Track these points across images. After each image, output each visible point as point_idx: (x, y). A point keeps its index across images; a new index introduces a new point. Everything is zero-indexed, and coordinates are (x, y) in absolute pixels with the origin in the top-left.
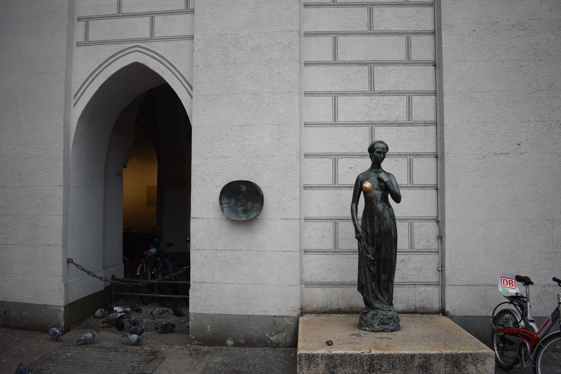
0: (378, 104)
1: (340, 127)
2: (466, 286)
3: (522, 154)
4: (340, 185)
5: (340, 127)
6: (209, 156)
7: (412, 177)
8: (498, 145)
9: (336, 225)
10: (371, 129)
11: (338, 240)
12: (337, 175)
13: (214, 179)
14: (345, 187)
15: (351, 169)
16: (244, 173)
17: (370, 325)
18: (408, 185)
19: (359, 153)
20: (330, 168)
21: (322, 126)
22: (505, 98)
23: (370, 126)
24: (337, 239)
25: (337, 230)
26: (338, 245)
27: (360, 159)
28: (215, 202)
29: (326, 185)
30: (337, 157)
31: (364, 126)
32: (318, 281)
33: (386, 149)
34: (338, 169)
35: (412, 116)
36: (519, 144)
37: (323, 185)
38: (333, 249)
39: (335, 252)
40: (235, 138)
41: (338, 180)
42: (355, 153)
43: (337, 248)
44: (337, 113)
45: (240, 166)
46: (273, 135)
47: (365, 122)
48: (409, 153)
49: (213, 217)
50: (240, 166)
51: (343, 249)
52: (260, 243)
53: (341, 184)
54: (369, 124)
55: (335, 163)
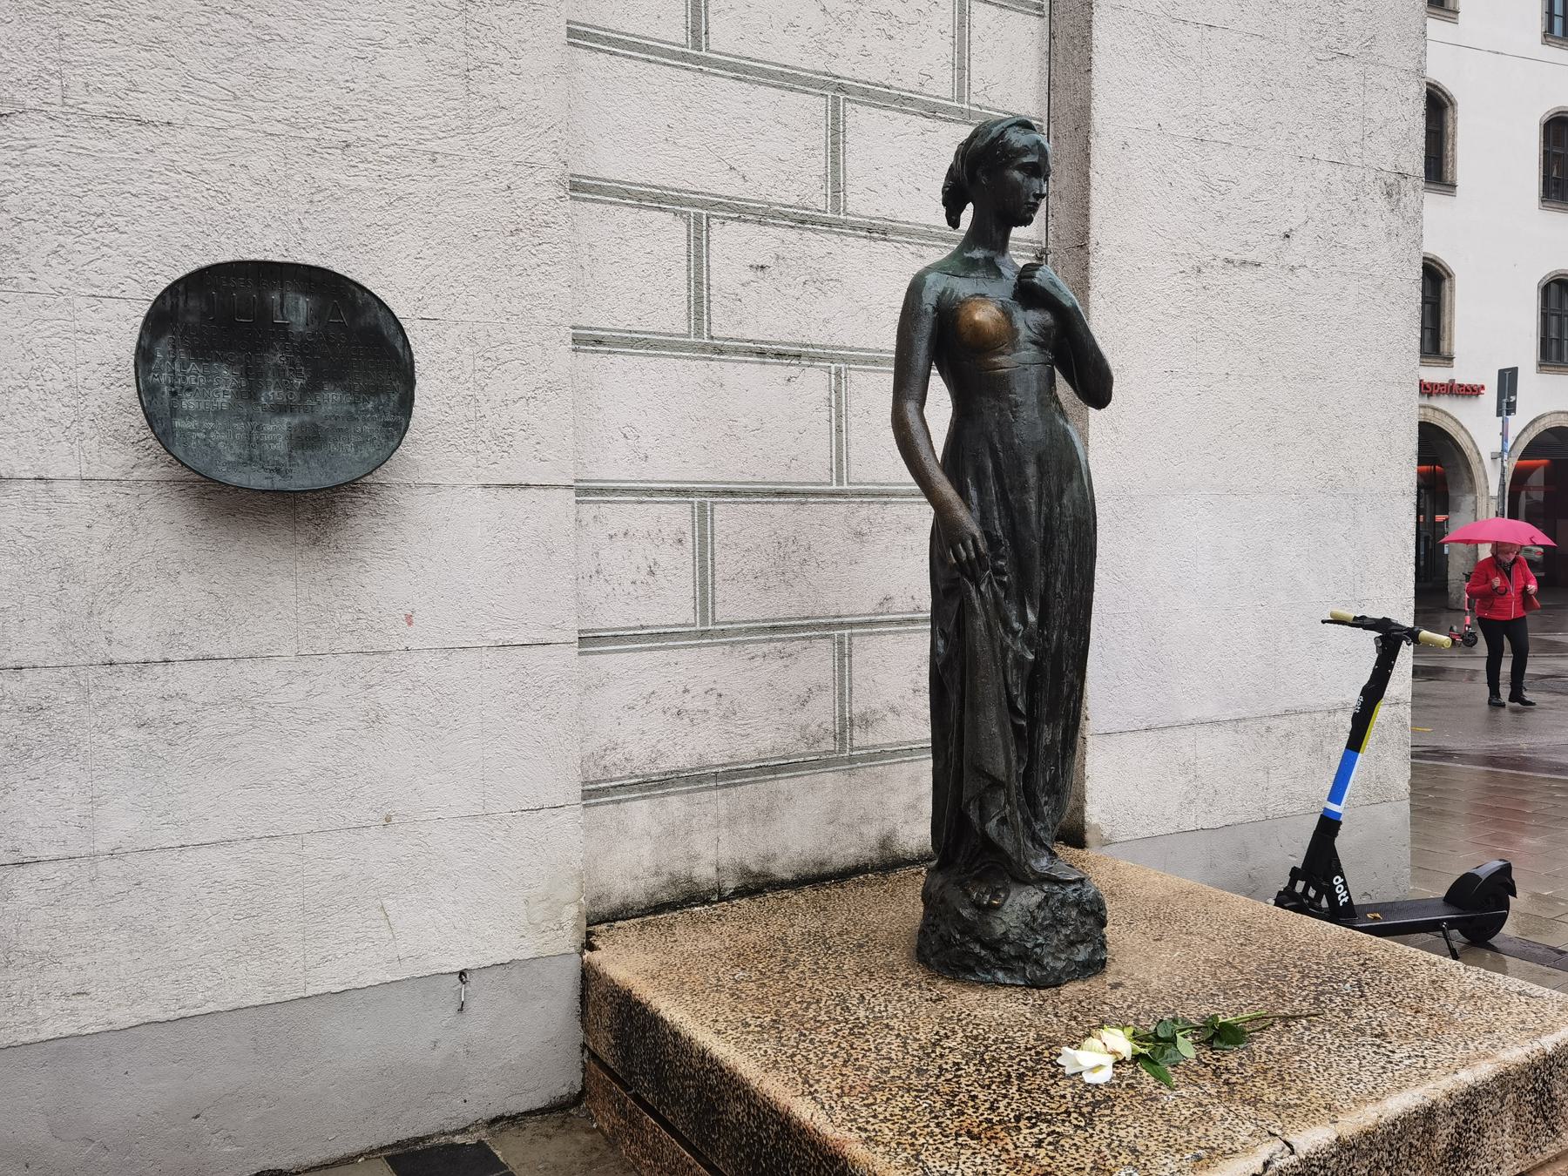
0: (858, 6)
1: (716, 75)
2: (1143, 733)
3: (1292, 269)
5: (716, 75)
6: (31, 103)
8: (1236, 231)
9: (703, 518)
11: (713, 584)
13: (78, 247)
14: (736, 351)
15: (759, 273)
16: (267, 231)
17: (1018, 958)
19: (791, 207)
20: (676, 258)
21: (643, 56)
22: (1261, 64)
23: (830, 94)
24: (709, 577)
25: (709, 540)
26: (713, 603)
27: (792, 235)
28: (88, 383)
29: (660, 334)
30: (704, 212)
31: (807, 89)
32: (638, 772)
34: (708, 266)
35: (969, 84)
36: (1288, 236)
37: (648, 336)
38: (694, 625)
39: (703, 634)
40: (203, 20)
43: (710, 620)
44: (706, 7)
45: (247, 185)
46: (431, 46)
47: (810, 75)
49: (74, 473)
50: (247, 185)
51: (731, 619)
52: (376, 613)
53: (721, 334)
54: (825, 85)
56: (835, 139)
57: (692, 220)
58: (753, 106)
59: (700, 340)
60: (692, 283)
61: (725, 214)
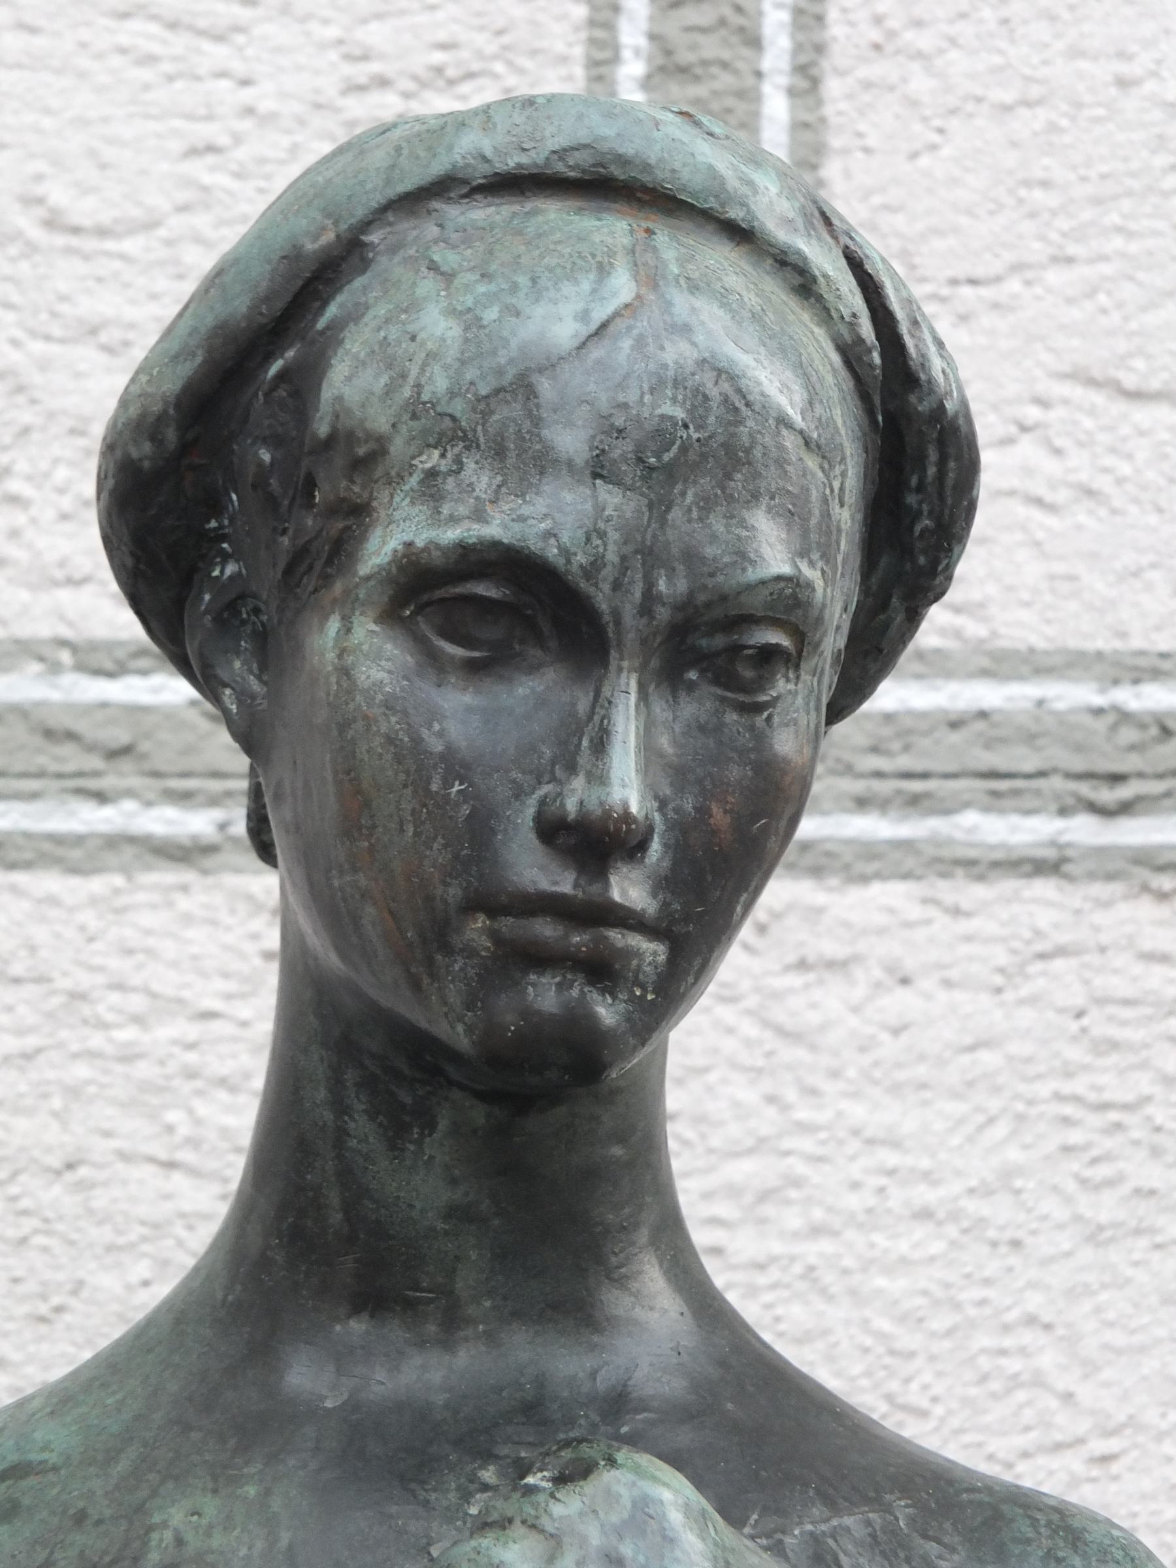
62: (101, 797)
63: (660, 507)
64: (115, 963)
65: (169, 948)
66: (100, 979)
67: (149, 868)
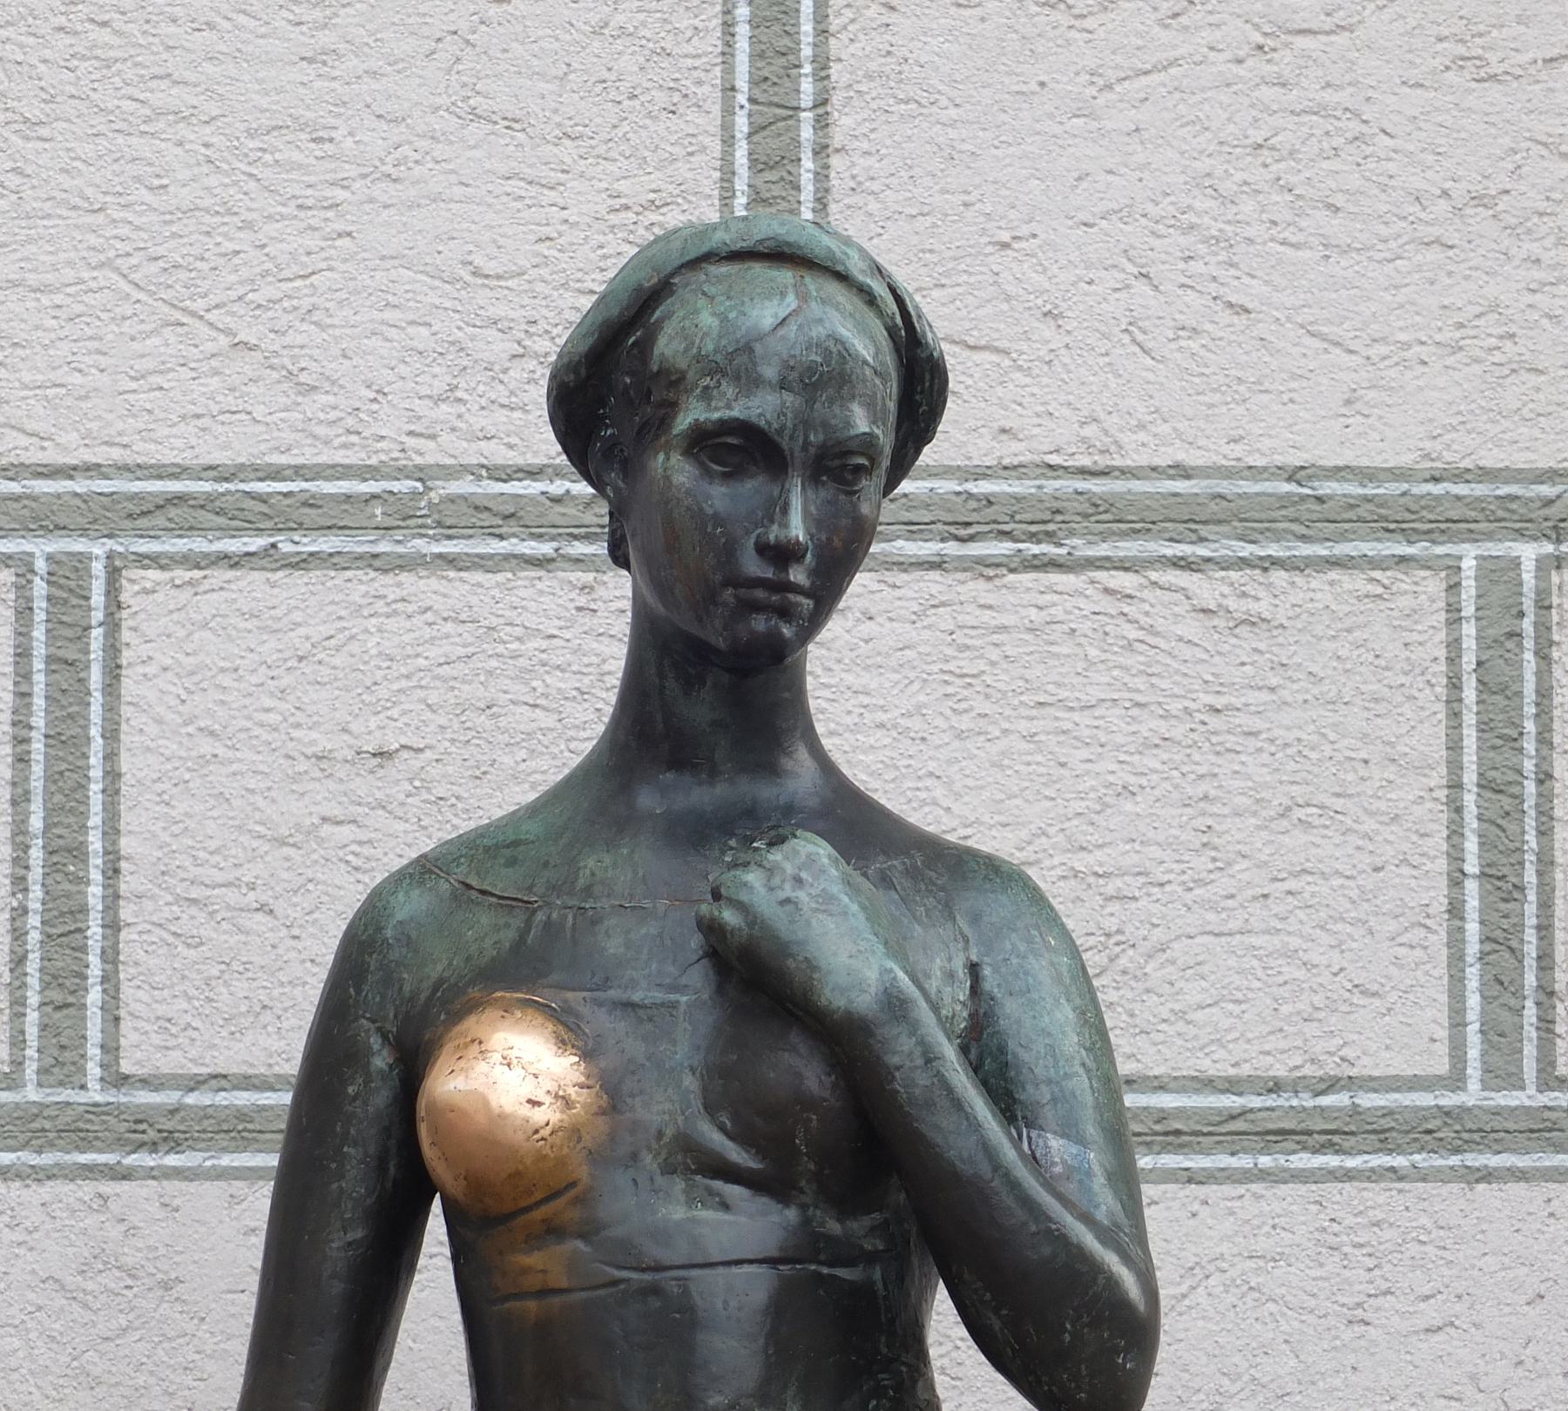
4: (145, 1082)
7: (1531, 949)
10: (754, 23)
12: (95, 893)
15: (364, 786)
18: (1449, 1100)
30: (99, 549)
33: (889, 392)
34: (113, 776)
41: (110, 980)
42: (451, 473)
48: (1486, 474)
53: (169, 1063)
55: (66, 665)
56: (771, 144)
57: (40, 588)
58: (353, 62)
59: (66, 1095)
60: (36, 854)
61: (199, 545)
62: (501, 537)
63: (811, 402)
64: (508, 613)
65: (532, 606)
66: (502, 621)
67: (524, 569)
